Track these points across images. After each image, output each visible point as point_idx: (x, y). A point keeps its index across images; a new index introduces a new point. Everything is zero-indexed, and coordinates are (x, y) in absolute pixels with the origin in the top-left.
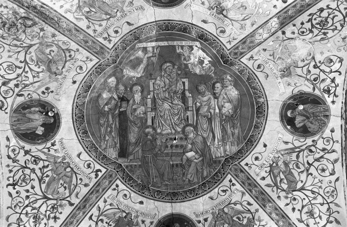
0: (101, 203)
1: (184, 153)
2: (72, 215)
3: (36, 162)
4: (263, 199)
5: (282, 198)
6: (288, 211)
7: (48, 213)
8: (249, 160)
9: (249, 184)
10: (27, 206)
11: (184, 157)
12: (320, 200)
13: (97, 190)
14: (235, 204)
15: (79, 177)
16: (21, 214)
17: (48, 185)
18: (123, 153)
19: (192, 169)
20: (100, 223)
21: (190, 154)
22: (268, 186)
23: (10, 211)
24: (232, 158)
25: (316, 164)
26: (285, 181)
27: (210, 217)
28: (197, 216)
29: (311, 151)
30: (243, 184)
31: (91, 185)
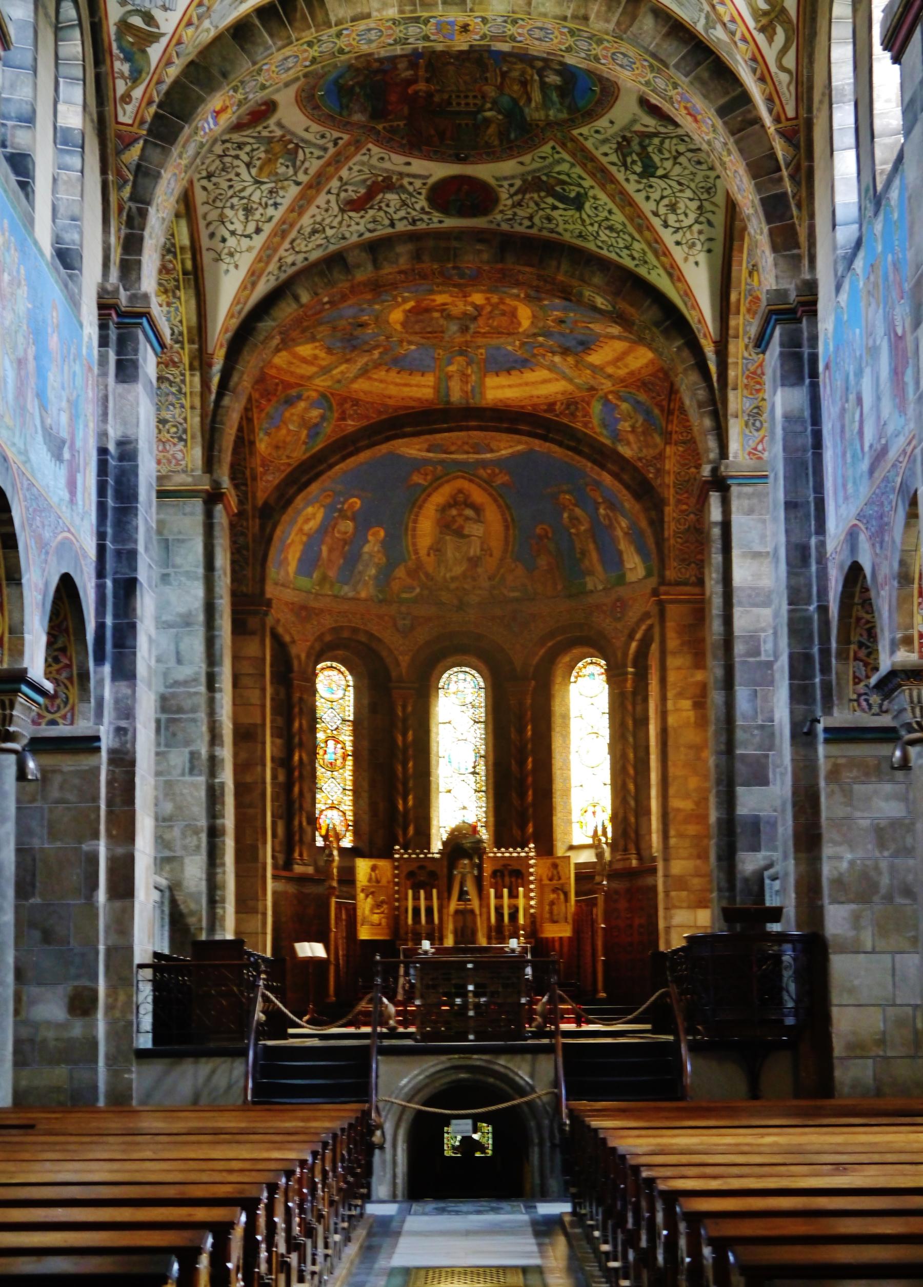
0: (344, 173)
2: (302, 196)
4: (604, 177)
5: (632, 181)
6: (639, 198)
7: (264, 200)
8: (585, 130)
9: (584, 157)
10: (231, 197)
11: (480, 116)
13: (338, 161)
14: (559, 173)
15: (307, 151)
16: (224, 207)
17: (261, 169)
18: (377, 114)
19: (492, 129)
20: (343, 195)
21: (489, 114)
22: (613, 164)
23: (207, 208)
25: (689, 155)
26: (639, 164)
27: (518, 183)
28: (497, 179)
29: (683, 140)
30: (573, 155)
31: (328, 156)
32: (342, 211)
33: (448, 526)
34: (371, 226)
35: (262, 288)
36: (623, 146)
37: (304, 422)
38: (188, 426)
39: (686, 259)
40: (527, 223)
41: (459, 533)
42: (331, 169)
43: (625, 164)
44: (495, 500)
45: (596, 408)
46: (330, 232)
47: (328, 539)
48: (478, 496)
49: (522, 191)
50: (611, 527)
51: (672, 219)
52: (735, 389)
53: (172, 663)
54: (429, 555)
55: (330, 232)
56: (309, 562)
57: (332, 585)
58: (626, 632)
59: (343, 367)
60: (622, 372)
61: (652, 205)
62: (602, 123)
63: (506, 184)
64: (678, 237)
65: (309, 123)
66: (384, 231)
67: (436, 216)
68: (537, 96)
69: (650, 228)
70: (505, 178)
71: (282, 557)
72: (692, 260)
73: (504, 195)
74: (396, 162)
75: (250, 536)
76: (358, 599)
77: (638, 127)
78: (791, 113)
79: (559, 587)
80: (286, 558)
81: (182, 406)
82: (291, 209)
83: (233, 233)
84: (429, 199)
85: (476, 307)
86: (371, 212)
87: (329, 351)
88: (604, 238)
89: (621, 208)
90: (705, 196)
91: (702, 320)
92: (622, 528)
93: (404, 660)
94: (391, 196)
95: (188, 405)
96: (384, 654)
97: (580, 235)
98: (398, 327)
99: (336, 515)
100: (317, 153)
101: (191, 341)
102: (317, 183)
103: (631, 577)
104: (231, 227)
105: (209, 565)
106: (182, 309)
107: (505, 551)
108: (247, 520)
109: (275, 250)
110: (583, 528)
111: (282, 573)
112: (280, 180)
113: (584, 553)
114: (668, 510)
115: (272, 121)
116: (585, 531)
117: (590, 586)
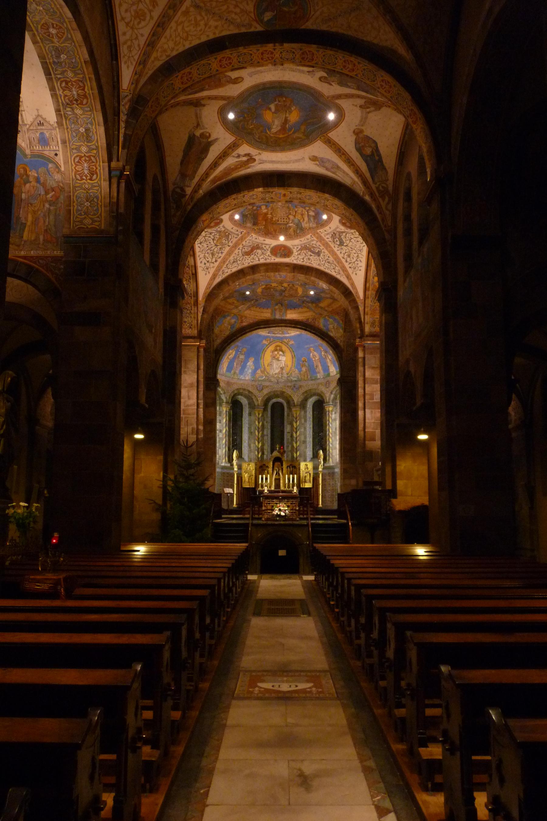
0: (244, 243)
1: (287, 224)
3: (211, 234)
4: (327, 246)
6: (338, 253)
8: (321, 230)
9: (320, 239)
12: (354, 251)
13: (242, 239)
17: (217, 241)
18: (255, 224)
19: (292, 230)
20: (243, 250)
21: (290, 225)
23: (200, 253)
24: (313, 228)
25: (355, 239)
27: (300, 247)
30: (317, 238)
32: (243, 255)
33: (274, 357)
34: (252, 260)
35: (218, 280)
36: (334, 235)
37: (230, 324)
38: (193, 323)
39: (353, 273)
40: (302, 260)
42: (240, 241)
43: (334, 242)
45: (322, 321)
46: (239, 262)
47: (236, 361)
49: (301, 250)
51: (348, 259)
52: (367, 314)
53: (187, 399)
55: (239, 262)
56: (229, 369)
57: (237, 375)
59: (242, 306)
60: (330, 309)
61: (342, 255)
62: (327, 228)
63: (295, 247)
64: (350, 265)
65: (233, 226)
66: (256, 262)
67: (273, 258)
68: (306, 219)
69: (341, 263)
70: (295, 246)
72: (354, 273)
73: (295, 251)
74: (260, 239)
77: (338, 230)
78: (390, 224)
81: (191, 317)
82: (227, 255)
83: (208, 262)
84: (271, 252)
85: (285, 288)
86: (252, 256)
87: (238, 301)
88: (326, 265)
89: (333, 256)
90: (359, 252)
91: (357, 293)
93: (260, 399)
94: (259, 251)
95: (193, 317)
96: (253, 397)
97: (319, 265)
98: (260, 294)
100: (235, 236)
101: (194, 296)
102: (236, 245)
103: (332, 374)
104: (208, 260)
105: (198, 369)
106: (191, 286)
107: (292, 365)
109: (221, 268)
112: (223, 244)
113: (317, 366)
115: (221, 225)
117: (318, 377)
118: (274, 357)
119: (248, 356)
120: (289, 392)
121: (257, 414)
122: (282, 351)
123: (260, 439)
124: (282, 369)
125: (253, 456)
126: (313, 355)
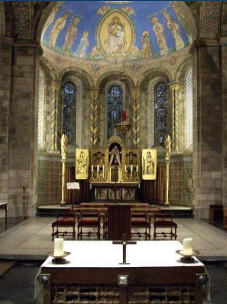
33: (111, 33)
41: (116, 35)
44: (129, 22)
48: (123, 20)
50: (172, 29)
54: (104, 43)
58: (176, 69)
71: (50, 37)
75: (30, 16)
76: (79, 58)
79: (151, 55)
80: (51, 38)
92: (176, 29)
93: (95, 80)
96: (88, 78)
99: (71, 24)
103: (178, 48)
107: (132, 42)
108: (29, 9)
110: (160, 32)
111: (50, 43)
113: (160, 42)
114: (202, 8)
116: (162, 33)
118: (111, 33)
119: (81, 29)
120: (128, 72)
121: (92, 97)
122: (122, 26)
123: (96, 125)
124: (121, 46)
125: (87, 143)
126: (156, 28)
